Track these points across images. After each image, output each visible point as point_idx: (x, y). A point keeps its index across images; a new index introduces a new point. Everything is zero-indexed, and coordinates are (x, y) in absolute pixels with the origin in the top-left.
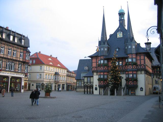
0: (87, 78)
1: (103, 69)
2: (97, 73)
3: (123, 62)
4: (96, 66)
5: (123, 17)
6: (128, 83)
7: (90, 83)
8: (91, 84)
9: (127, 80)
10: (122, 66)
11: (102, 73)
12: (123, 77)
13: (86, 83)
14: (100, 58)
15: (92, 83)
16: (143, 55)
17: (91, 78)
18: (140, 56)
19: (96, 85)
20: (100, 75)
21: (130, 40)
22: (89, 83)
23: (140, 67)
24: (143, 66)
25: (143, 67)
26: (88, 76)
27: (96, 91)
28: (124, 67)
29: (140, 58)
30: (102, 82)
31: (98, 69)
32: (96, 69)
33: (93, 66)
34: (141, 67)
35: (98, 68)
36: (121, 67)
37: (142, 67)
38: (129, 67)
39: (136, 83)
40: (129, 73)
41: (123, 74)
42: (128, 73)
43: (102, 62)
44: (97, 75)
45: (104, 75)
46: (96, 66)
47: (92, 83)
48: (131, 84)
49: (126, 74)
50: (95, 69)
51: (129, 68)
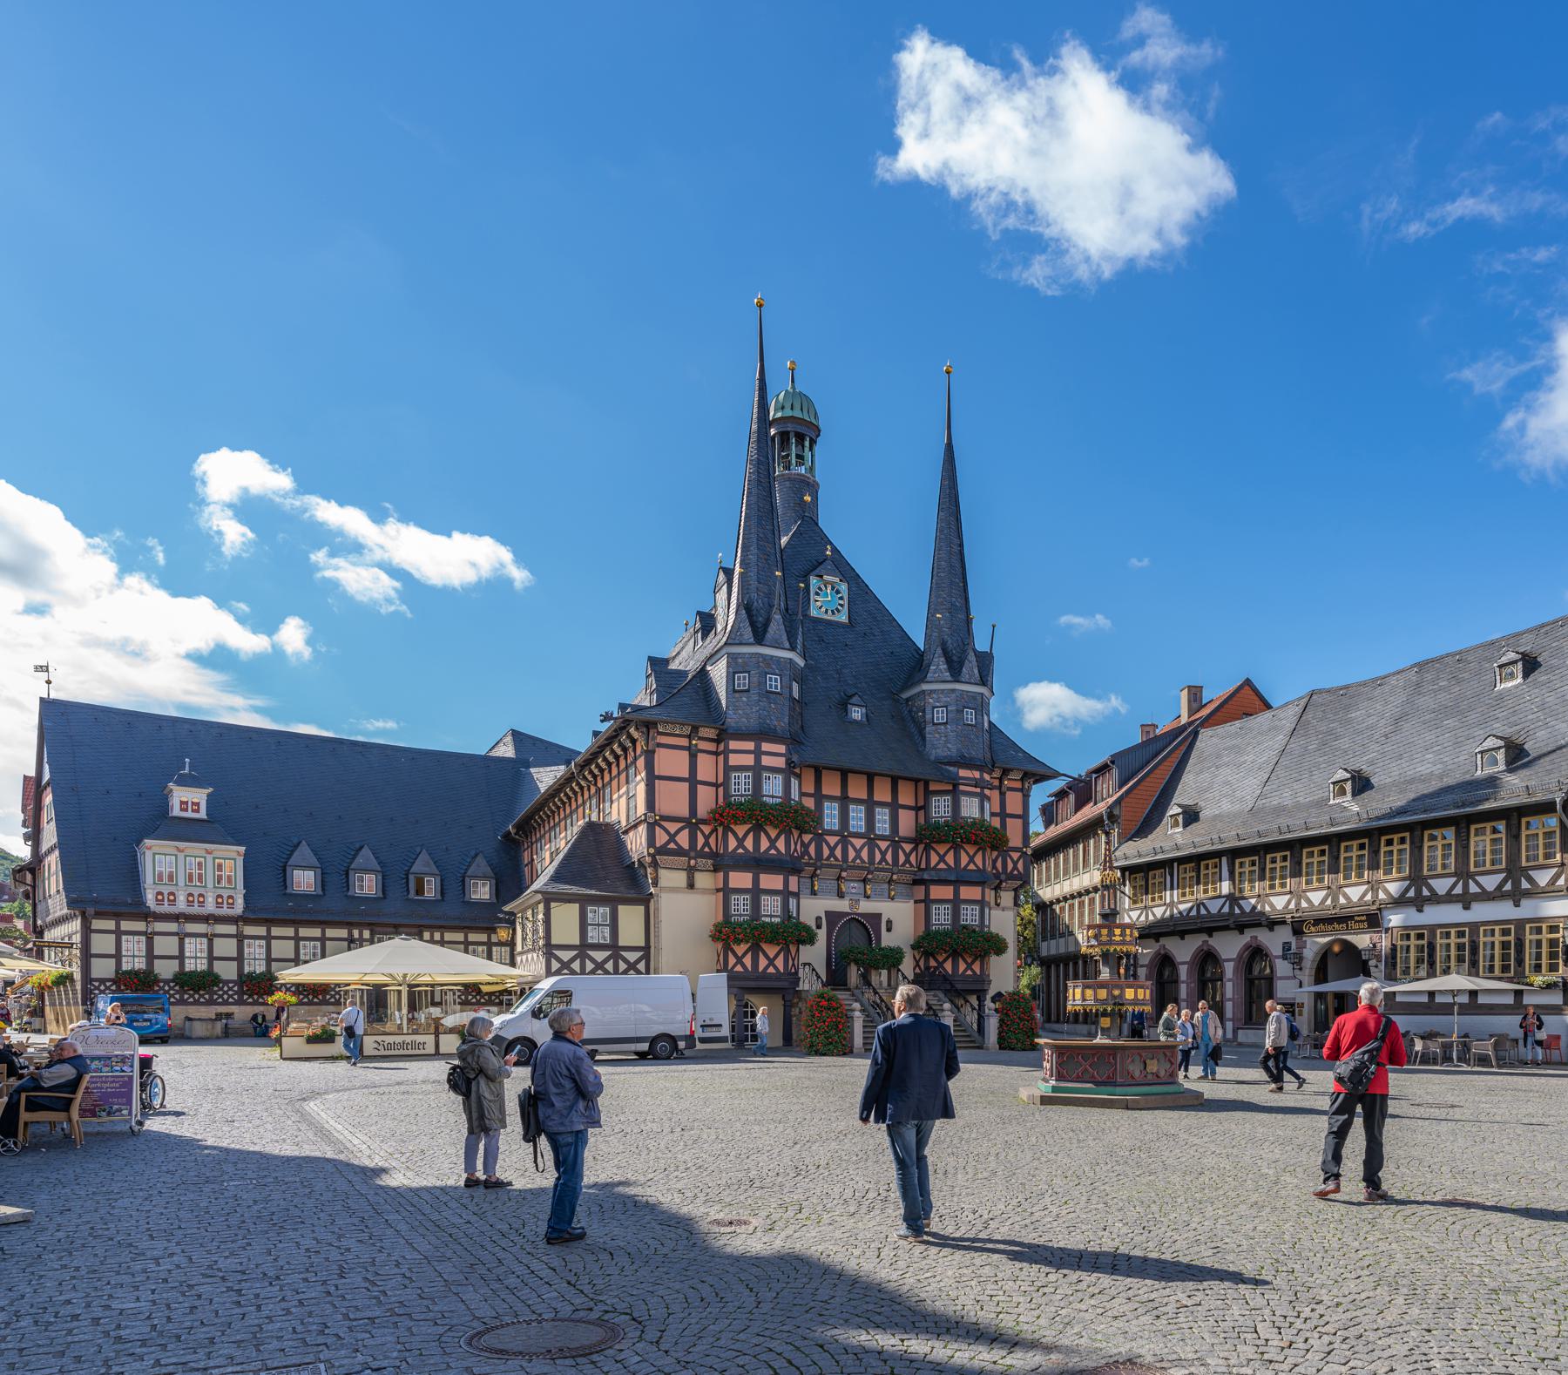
2: (691, 871)
4: (685, 812)
11: (772, 881)
12: (889, 922)
14: (758, 753)
16: (1018, 785)
17: (623, 910)
18: (1002, 794)
21: (949, 661)
23: (999, 865)
24: (1015, 855)
25: (1015, 863)
28: (908, 847)
31: (707, 838)
32: (693, 839)
33: (665, 805)
35: (707, 829)
36: (883, 845)
37: (1010, 866)
38: (934, 859)
40: (967, 892)
42: (957, 893)
44: (691, 886)
49: (927, 902)
50: (683, 839)
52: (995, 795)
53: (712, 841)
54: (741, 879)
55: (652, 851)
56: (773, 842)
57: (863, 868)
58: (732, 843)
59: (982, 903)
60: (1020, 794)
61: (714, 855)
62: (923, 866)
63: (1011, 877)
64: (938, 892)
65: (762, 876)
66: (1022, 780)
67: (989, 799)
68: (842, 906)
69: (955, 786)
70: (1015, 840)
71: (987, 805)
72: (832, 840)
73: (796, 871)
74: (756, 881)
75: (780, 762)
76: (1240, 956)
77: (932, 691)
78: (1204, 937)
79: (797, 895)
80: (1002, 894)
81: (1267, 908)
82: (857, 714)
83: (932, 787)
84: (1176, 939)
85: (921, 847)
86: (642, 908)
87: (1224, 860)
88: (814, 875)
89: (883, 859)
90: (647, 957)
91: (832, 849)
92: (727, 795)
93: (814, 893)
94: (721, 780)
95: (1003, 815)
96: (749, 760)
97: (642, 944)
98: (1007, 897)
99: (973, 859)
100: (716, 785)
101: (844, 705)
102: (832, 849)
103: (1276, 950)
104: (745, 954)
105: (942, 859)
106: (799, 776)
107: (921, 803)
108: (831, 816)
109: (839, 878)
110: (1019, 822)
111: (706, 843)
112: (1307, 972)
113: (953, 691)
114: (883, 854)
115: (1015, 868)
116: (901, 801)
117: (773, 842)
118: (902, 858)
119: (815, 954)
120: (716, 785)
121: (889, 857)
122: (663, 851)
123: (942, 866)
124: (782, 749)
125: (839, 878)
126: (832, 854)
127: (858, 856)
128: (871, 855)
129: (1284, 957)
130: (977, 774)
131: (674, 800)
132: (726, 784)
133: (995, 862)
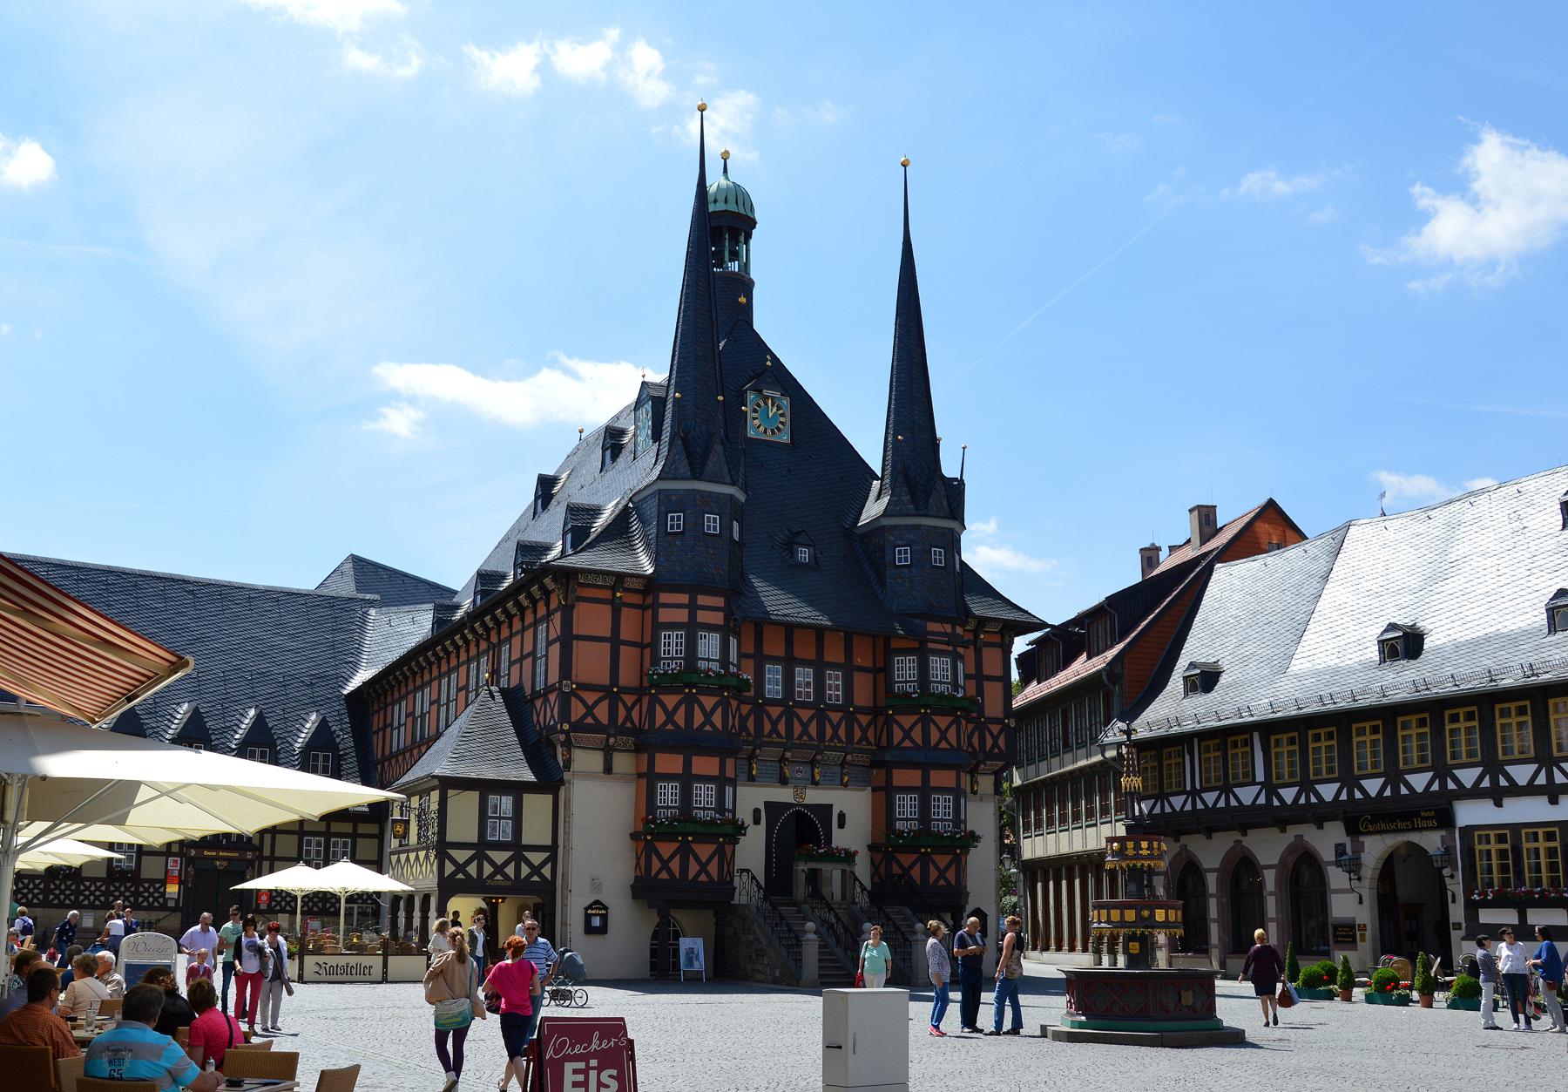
0: (474, 796)
1: (717, 719)
2: (608, 752)
3: (857, 675)
4: (606, 681)
5: (735, 256)
6: (916, 873)
7: (518, 858)
8: (525, 870)
9: (886, 844)
10: (847, 709)
12: (842, 816)
13: (461, 856)
14: (693, 607)
15: (536, 858)
18: (978, 652)
19: (596, 884)
20: (687, 780)
22: (499, 857)
23: (975, 741)
24: (995, 729)
25: (995, 739)
26: (490, 774)
27: (596, 940)
28: (864, 719)
29: (979, 664)
30: (704, 851)
31: (629, 710)
32: (613, 712)
34: (982, 741)
36: (835, 717)
37: (989, 742)
39: (951, 875)
40: (939, 778)
41: (845, 785)
42: (926, 779)
43: (709, 646)
44: (608, 769)
45: (722, 781)
46: (606, 681)
47: (536, 858)
48: (942, 882)
50: (602, 712)
51: (933, 742)
52: (969, 653)
53: (635, 714)
54: (669, 763)
55: (566, 727)
56: (708, 716)
57: (810, 747)
58: (660, 717)
59: (957, 792)
60: (999, 651)
61: (636, 732)
62: (884, 743)
63: (991, 756)
64: (902, 777)
65: (695, 759)
66: (1001, 633)
67: (962, 658)
68: (785, 795)
69: (923, 643)
70: (993, 708)
71: (960, 666)
72: (775, 711)
73: (733, 752)
74: (687, 765)
75: (718, 618)
76: (1283, 860)
77: (892, 527)
78: (1236, 835)
79: (734, 783)
80: (981, 779)
81: (1313, 800)
82: (804, 554)
83: (894, 645)
84: (1201, 838)
85: (881, 719)
86: (549, 798)
87: (1256, 736)
88: (751, 757)
89: (835, 735)
90: (553, 859)
91: (774, 723)
92: (655, 660)
93: (751, 779)
94: (647, 639)
95: (979, 677)
96: (682, 616)
97: (548, 842)
98: (986, 783)
99: (945, 732)
100: (640, 645)
101: (790, 546)
102: (774, 723)
103: (1327, 854)
104: (673, 856)
105: (907, 734)
106: (738, 635)
107: (880, 665)
108: (773, 685)
109: (782, 760)
110: (999, 686)
111: (629, 718)
112: (1366, 883)
113: (918, 526)
114: (835, 728)
115: (995, 744)
116: (858, 661)
117: (708, 716)
118: (858, 734)
119: (752, 851)
120: (640, 645)
121: (842, 732)
122: (578, 727)
123: (907, 743)
124: (719, 601)
125: (782, 760)
126: (774, 730)
127: (805, 732)
129: (1338, 864)
130: (948, 628)
131: (592, 663)
132: (654, 644)
133: (970, 737)
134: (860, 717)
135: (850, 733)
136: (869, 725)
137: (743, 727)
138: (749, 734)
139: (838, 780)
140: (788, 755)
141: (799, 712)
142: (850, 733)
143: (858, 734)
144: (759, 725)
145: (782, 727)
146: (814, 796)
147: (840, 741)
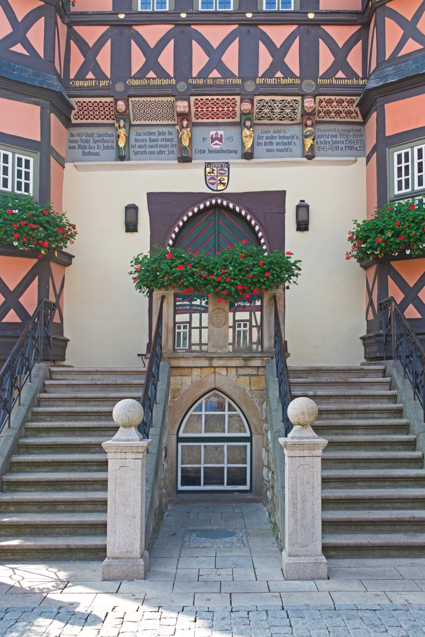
68: (189, 179)
72: (152, 34)
91: (152, 54)
102: (152, 54)
114: (279, 54)
118: (326, 59)
121: (292, 59)
128: (249, 58)
134: (329, 29)
135: (309, 59)
136: (350, 44)
137: (90, 64)
138: (100, 75)
139: (297, 149)
140: (182, 106)
141: (204, 30)
142: (309, 59)
143: (326, 59)
144: (121, 59)
145: (167, 59)
146: (245, 179)
147: (287, 73)
